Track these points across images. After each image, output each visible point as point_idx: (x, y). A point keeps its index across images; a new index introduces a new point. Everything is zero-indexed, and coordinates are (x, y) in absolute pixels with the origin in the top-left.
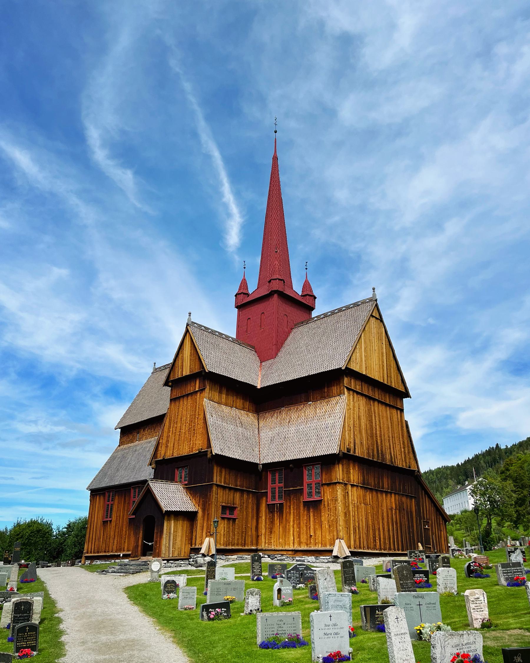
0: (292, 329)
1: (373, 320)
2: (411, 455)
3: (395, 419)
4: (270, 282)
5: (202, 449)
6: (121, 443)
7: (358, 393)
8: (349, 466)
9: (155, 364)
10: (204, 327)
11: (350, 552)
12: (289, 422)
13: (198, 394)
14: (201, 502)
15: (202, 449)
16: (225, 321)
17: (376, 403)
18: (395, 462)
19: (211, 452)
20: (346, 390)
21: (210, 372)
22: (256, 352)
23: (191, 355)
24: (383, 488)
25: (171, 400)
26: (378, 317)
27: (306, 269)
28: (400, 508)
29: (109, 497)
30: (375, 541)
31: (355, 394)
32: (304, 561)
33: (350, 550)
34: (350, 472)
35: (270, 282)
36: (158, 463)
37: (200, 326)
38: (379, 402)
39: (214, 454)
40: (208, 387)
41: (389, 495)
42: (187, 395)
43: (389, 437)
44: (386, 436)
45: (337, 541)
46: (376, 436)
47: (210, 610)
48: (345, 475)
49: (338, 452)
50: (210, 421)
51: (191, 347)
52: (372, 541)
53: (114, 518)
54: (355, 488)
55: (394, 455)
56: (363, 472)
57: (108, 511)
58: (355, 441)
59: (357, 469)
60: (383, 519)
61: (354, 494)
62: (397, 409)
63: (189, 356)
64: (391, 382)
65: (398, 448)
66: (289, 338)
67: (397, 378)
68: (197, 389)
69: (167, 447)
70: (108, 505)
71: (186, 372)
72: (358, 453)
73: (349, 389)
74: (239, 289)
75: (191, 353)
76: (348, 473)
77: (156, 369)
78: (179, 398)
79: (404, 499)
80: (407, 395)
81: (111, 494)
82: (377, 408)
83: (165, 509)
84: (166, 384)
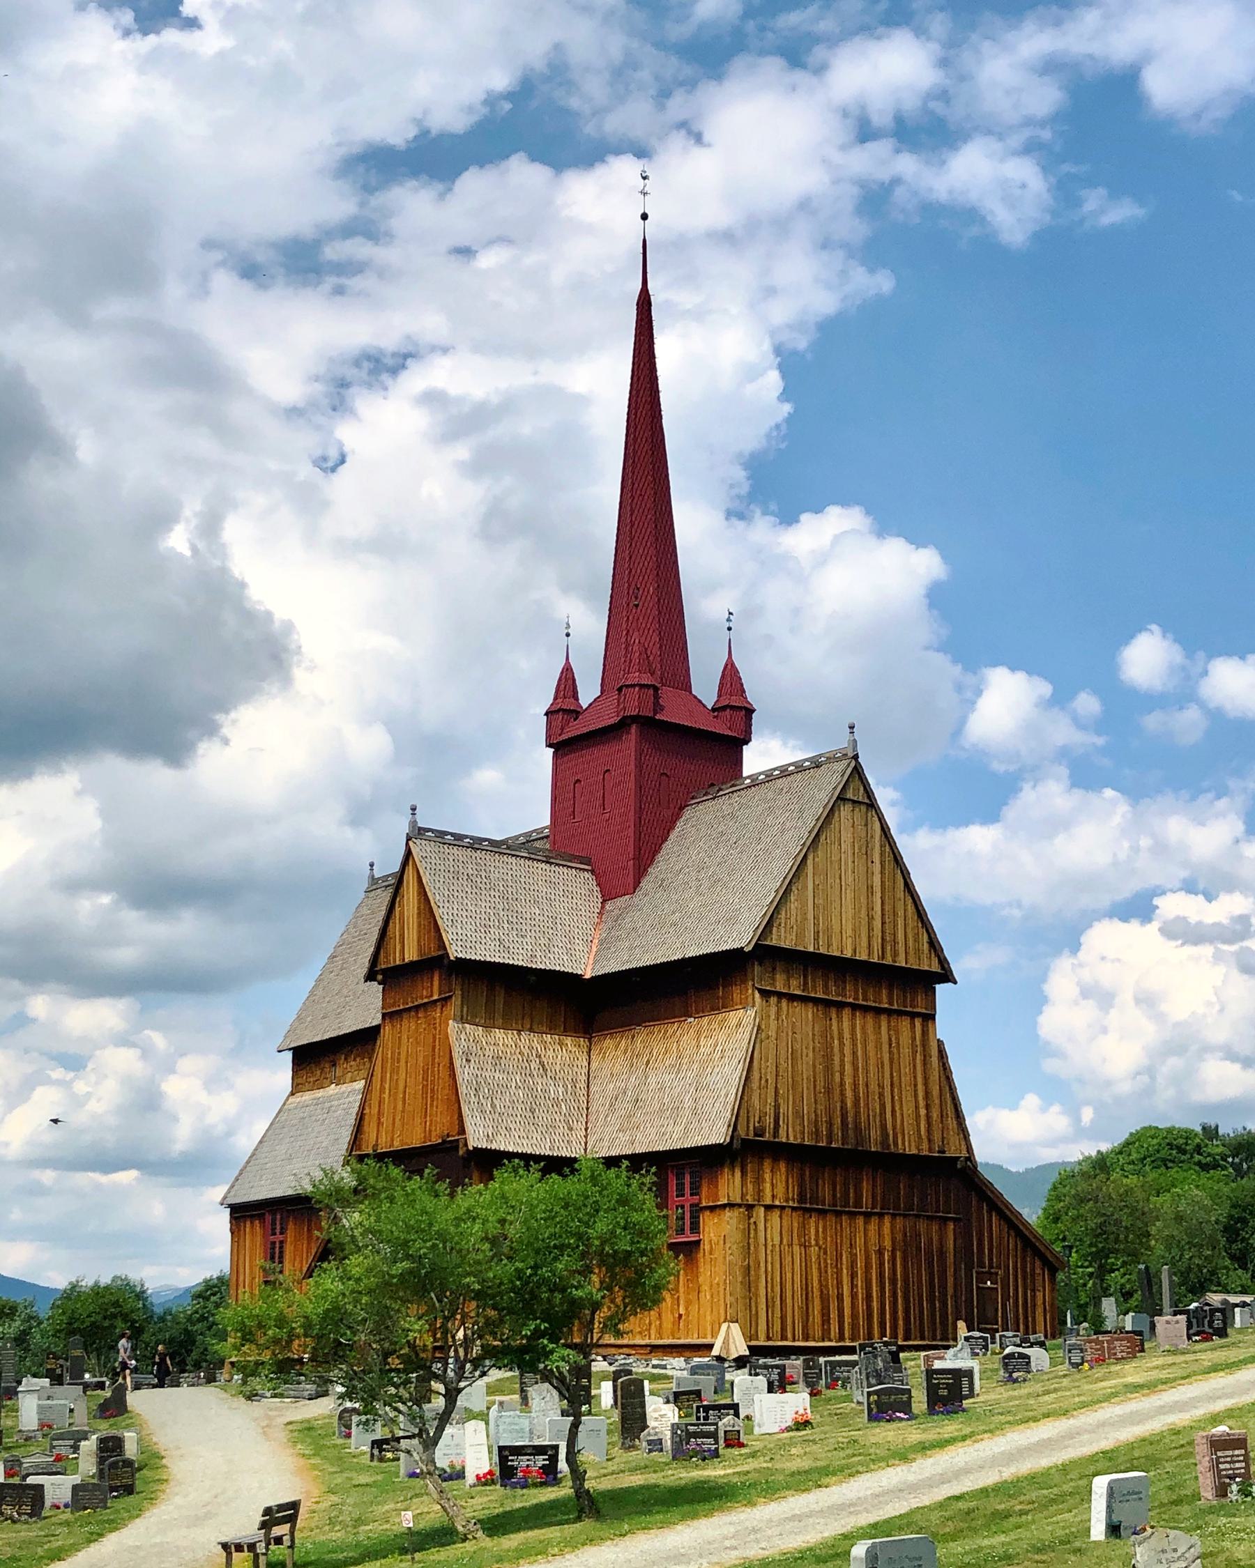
0: (682, 808)
1: (845, 811)
2: (951, 1123)
4: (620, 690)
5: (448, 1136)
6: (296, 1089)
7: (792, 998)
8: (761, 1164)
10: (452, 834)
11: (749, 1347)
12: (648, 1062)
15: (448, 1136)
16: (516, 789)
17: (846, 1013)
18: (896, 1144)
19: (466, 1145)
20: (757, 995)
22: (593, 872)
23: (419, 914)
24: (858, 1203)
26: (861, 797)
27: (729, 629)
28: (908, 1247)
29: (274, 1223)
30: (826, 1320)
31: (784, 1003)
32: (664, 1367)
33: (753, 1343)
34: (764, 1181)
35: (620, 690)
36: (361, 1159)
38: (855, 1007)
40: (459, 992)
41: (874, 1221)
43: (881, 1086)
44: (873, 1087)
45: (724, 1326)
46: (842, 1094)
48: (750, 1186)
49: (728, 1140)
50: (464, 1074)
51: (419, 894)
52: (818, 1319)
54: (777, 1213)
55: (894, 1128)
56: (802, 1176)
58: (777, 1107)
59: (783, 1170)
60: (853, 1276)
61: (772, 1228)
62: (913, 1015)
64: (895, 954)
65: (908, 1109)
66: (673, 836)
67: (916, 940)
68: (435, 997)
69: (379, 1123)
70: (274, 1243)
71: (411, 955)
72: (789, 1134)
73: (765, 994)
75: (419, 908)
76: (759, 1180)
77: (373, 880)
79: (922, 1226)
80: (946, 976)
81: (278, 1217)
82: (844, 1023)
84: (370, 977)
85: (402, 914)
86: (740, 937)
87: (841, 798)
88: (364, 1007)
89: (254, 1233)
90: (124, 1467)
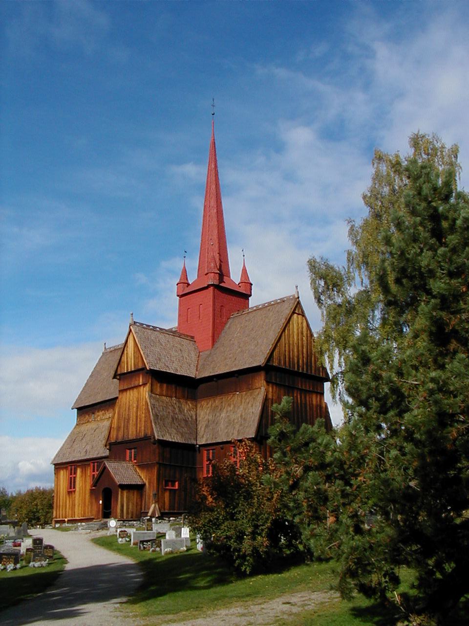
3: (314, 403)
9: (105, 344)
12: (221, 409)
13: (142, 388)
14: (148, 477)
21: (150, 369)
25: (120, 391)
36: (111, 444)
37: (142, 324)
39: (156, 437)
42: (132, 388)
47: (145, 543)
53: (77, 489)
57: (72, 483)
62: (317, 393)
63: (133, 347)
68: (141, 384)
71: (132, 368)
74: (180, 280)
75: (134, 350)
78: (126, 390)
83: (118, 484)
84: (114, 377)
85: (127, 353)
86: (260, 361)
87: (294, 313)
88: (111, 389)
89: (63, 474)
90: (50, 548)
